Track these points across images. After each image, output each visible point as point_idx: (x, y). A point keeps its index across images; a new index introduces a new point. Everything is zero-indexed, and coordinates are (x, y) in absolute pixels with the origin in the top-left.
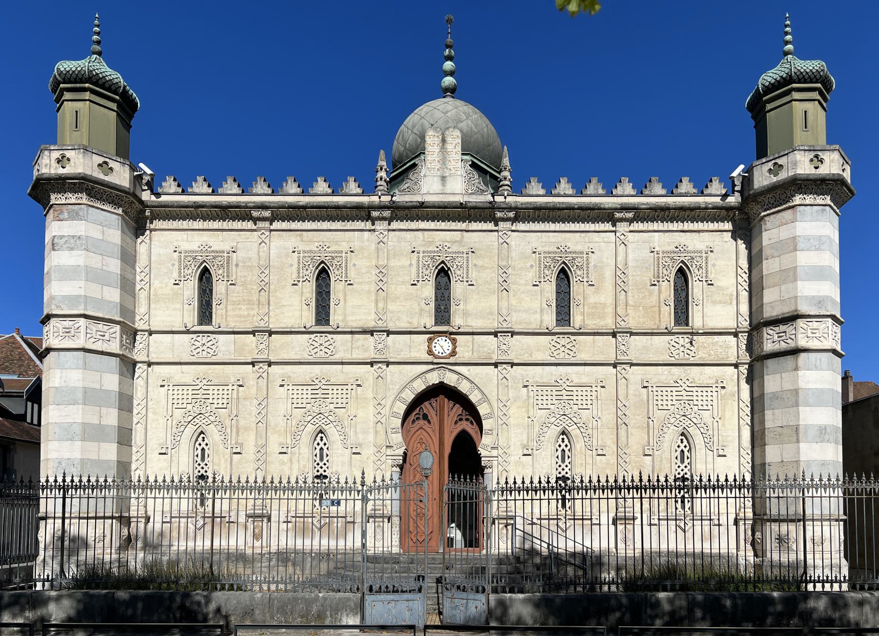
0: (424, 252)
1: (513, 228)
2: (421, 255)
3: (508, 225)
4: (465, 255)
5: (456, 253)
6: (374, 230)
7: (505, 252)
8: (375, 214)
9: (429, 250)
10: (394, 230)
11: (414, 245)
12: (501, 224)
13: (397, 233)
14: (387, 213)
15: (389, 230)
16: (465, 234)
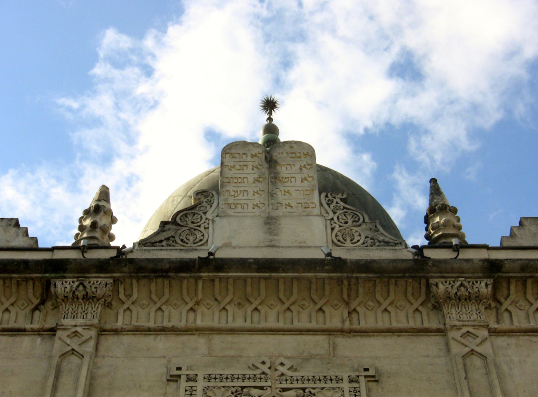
0: (209, 378)
1: (493, 325)
2: (201, 384)
3: (471, 314)
4: (346, 386)
5: (314, 379)
6: (53, 331)
7: (477, 374)
8: (63, 286)
9: (228, 372)
10: (116, 332)
11: (177, 362)
12: (453, 315)
13: (126, 339)
14: (99, 284)
15: (102, 332)
16: (341, 341)
